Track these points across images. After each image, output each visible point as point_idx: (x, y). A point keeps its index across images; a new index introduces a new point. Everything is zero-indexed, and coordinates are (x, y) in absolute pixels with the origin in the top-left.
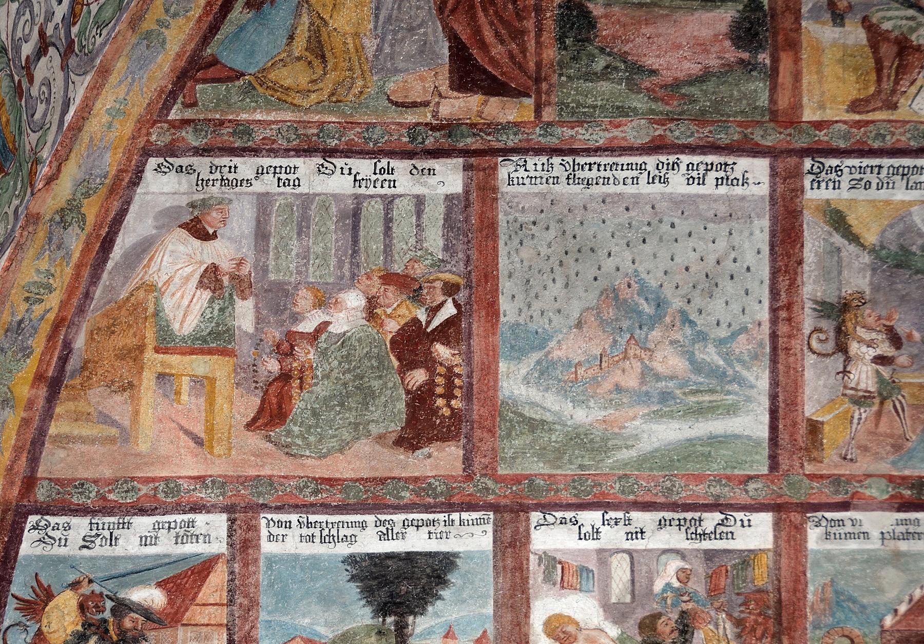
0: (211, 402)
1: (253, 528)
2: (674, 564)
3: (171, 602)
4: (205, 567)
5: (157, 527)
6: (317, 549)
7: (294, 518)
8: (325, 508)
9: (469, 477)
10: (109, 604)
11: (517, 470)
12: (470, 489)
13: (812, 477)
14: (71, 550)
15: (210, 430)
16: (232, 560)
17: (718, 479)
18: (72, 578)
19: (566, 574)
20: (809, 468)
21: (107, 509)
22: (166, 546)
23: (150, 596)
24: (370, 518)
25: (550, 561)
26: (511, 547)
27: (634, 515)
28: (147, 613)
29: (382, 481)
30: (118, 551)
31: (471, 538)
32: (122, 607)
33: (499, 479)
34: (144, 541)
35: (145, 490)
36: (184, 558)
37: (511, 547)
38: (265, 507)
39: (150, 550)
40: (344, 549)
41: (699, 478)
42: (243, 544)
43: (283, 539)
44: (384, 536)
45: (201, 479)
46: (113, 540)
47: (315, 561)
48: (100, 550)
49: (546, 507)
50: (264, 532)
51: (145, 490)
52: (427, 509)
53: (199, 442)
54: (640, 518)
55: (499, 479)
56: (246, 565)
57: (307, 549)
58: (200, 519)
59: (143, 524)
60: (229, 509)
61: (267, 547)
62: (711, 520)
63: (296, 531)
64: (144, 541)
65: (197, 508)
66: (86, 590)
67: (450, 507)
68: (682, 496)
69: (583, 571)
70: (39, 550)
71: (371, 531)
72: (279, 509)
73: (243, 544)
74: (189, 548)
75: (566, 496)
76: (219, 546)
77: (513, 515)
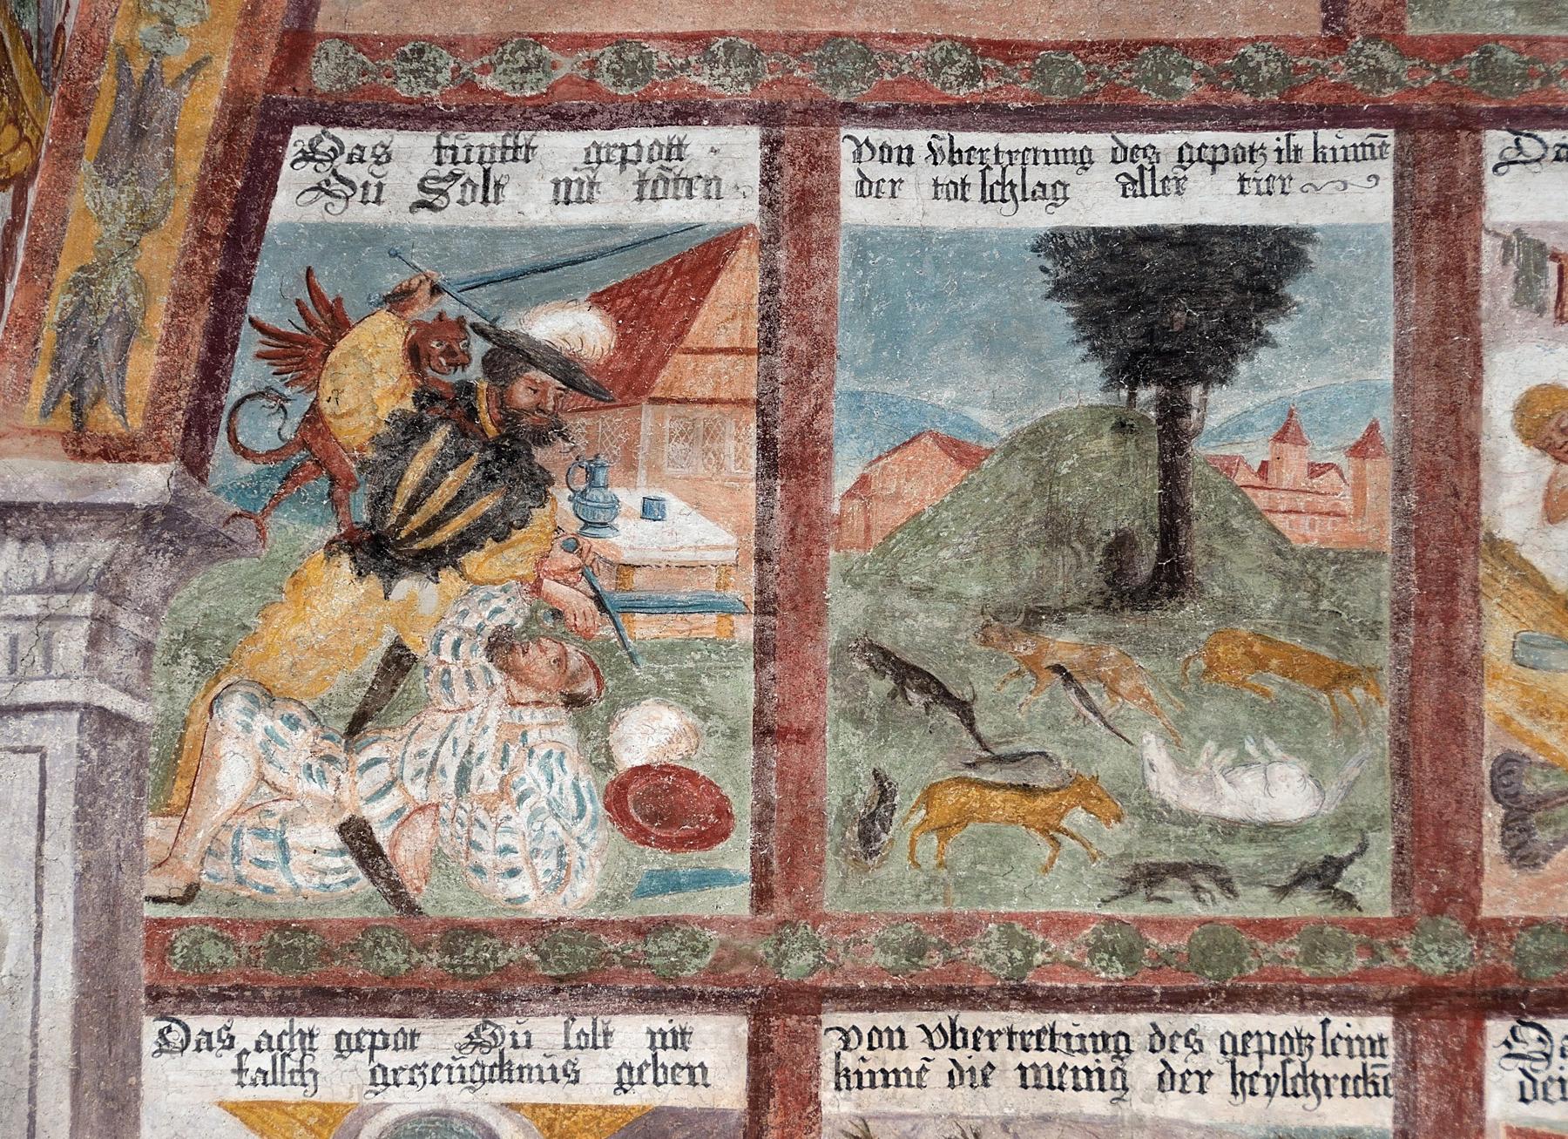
3: (625, 343)
6: (975, 216)
24: (1100, 142)
40: (1037, 218)
44: (1133, 186)
47: (968, 243)
57: (949, 217)
61: (855, 211)
63: (924, 172)
71: (1103, 174)
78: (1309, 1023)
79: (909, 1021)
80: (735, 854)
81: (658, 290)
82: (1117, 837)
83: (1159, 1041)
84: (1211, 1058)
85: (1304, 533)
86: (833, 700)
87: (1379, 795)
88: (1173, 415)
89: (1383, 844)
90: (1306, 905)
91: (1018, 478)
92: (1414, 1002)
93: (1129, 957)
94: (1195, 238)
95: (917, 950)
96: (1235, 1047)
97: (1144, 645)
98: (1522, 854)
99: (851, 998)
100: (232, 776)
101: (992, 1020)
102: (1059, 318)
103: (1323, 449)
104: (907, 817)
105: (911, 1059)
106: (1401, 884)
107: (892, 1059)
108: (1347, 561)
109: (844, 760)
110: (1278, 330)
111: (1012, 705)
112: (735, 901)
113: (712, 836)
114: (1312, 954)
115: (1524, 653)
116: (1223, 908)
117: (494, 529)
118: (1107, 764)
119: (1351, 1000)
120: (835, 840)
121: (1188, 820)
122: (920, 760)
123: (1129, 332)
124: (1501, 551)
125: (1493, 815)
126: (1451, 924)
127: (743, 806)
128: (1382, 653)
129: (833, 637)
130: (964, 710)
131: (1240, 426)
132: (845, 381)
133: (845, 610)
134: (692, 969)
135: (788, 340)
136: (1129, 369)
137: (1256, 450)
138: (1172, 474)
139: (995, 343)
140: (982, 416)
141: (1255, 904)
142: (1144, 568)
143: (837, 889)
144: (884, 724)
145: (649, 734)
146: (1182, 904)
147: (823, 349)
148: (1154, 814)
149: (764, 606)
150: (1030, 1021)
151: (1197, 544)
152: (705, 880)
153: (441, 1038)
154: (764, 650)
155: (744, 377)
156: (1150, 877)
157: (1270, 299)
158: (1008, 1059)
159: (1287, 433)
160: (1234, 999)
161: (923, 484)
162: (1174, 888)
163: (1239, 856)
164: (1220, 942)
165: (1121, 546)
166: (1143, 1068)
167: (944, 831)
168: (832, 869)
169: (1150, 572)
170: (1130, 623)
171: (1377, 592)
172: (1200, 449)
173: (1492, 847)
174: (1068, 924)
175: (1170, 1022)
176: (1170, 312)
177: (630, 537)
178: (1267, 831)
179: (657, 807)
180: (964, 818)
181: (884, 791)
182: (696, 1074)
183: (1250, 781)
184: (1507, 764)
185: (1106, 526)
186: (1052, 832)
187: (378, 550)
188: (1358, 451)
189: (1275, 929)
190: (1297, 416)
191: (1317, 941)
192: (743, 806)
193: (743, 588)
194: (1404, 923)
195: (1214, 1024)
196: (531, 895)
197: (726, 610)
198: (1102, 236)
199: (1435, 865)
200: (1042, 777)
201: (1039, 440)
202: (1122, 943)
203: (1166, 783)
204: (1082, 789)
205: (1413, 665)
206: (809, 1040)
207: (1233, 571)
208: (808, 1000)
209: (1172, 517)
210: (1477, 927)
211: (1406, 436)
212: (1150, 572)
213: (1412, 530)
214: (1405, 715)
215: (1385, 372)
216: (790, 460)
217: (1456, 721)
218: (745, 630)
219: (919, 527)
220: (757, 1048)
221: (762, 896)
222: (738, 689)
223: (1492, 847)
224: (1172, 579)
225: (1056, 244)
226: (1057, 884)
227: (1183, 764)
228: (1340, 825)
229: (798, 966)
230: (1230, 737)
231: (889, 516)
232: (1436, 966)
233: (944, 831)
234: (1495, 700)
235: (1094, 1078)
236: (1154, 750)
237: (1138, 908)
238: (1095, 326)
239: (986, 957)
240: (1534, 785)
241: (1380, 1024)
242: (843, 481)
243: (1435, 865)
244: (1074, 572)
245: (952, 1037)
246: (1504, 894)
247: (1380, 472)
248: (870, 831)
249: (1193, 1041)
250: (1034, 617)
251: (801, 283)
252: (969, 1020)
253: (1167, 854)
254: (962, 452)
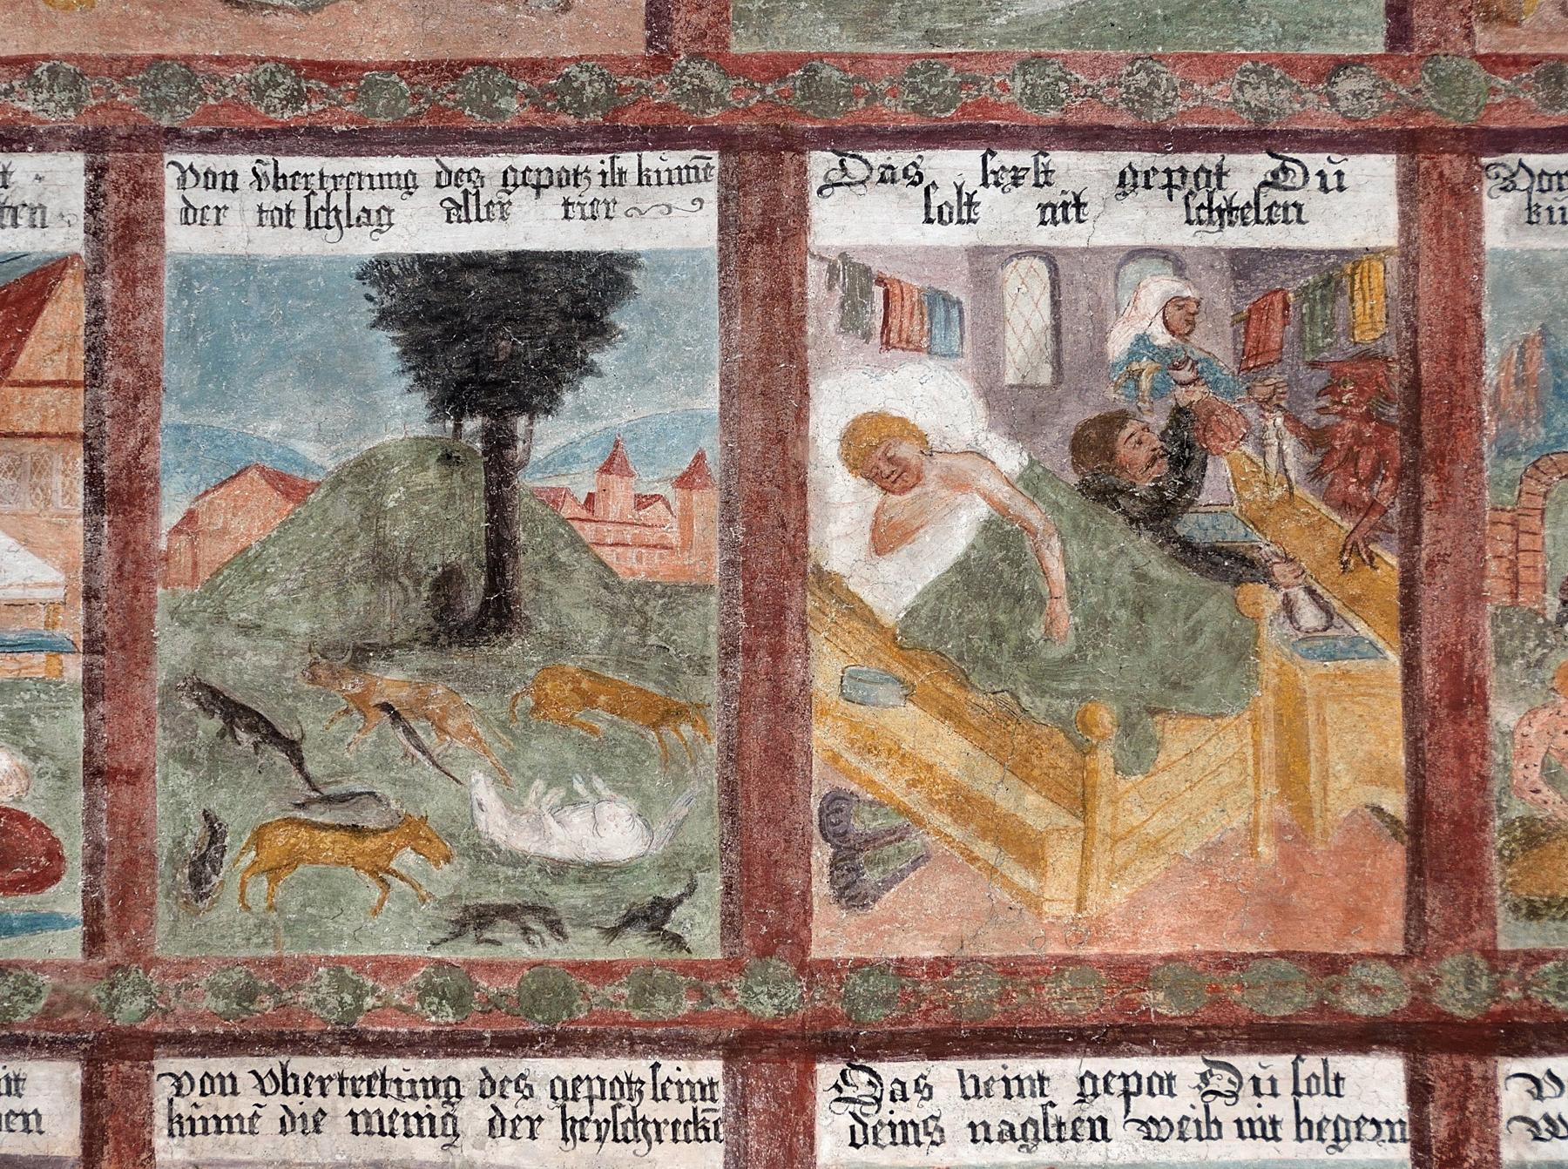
2: (1158, 287)
6: (299, 243)
7: (243, 163)
8: (319, 139)
9: (661, 62)
11: (775, 44)
12: (663, 91)
13: (1493, 62)
16: (95, 271)
17: (1263, 68)
19: (896, 312)
20: (1487, 40)
24: (424, 166)
25: (857, 277)
26: (763, 238)
27: (1060, 159)
29: (453, 70)
31: (667, 217)
33: (733, 67)
37: (763, 238)
38: (174, 136)
40: (363, 245)
41: (1217, 66)
43: (220, 217)
44: (457, 212)
47: (292, 271)
49: (845, 140)
50: (172, 201)
52: (562, 142)
54: (1076, 168)
55: (733, 67)
56: (129, 283)
60: (90, 142)
61: (180, 239)
62: (1246, 172)
63: (248, 199)
67: (614, 138)
68: (1174, 111)
69: (937, 301)
71: (428, 199)
72: (208, 142)
73: (123, 230)
75: (895, 111)
76: (65, 236)
77: (763, 156)
78: (640, 1067)
79: (240, 1067)
80: (67, 897)
82: (447, 878)
83: (490, 1086)
84: (542, 1103)
85: (631, 565)
86: (162, 741)
87: (707, 834)
88: (499, 445)
89: (712, 884)
90: (635, 947)
91: (344, 512)
92: (744, 1046)
93: (459, 1001)
94: (519, 265)
95: (248, 994)
96: (565, 1092)
97: (471, 681)
98: (851, 895)
99: (183, 1043)
101: (323, 1066)
102: (385, 348)
103: (649, 480)
104: (238, 859)
105: (243, 1105)
106: (730, 926)
107: (225, 1106)
108: (674, 595)
109: (175, 800)
110: (603, 358)
111: (341, 744)
112: (66, 945)
113: (44, 879)
114: (642, 996)
115: (852, 687)
116: (552, 951)
118: (435, 805)
119: (681, 1044)
120: (166, 881)
121: (517, 860)
122: (250, 800)
123: (455, 362)
124: (829, 583)
125: (821, 854)
126: (780, 966)
127: (74, 849)
128: (710, 690)
129: (161, 676)
130: (293, 749)
131: (566, 457)
132: (171, 414)
133: (173, 648)
134: (26, 1014)
135: (114, 371)
136: (454, 400)
137: (582, 483)
138: (498, 506)
139: (321, 374)
140: (309, 450)
141: (585, 946)
142: (471, 603)
143: (168, 932)
144: (213, 765)
146: (512, 947)
147: (149, 381)
148: (483, 854)
149: (92, 645)
150: (360, 1066)
151: (525, 576)
152: (37, 923)
154: (93, 690)
155: (70, 410)
156: (478, 919)
157: (595, 327)
158: (339, 1105)
159: (613, 464)
160: (563, 1043)
161: (250, 519)
162: (504, 930)
163: (568, 897)
164: (550, 985)
165: (447, 582)
166: (474, 1114)
167: (274, 872)
168: (164, 911)
169: (477, 608)
170: (458, 660)
171: (704, 626)
172: (527, 481)
173: (821, 887)
174: (397, 968)
175: (501, 1067)
176: (495, 340)
178: (596, 872)
180: (293, 859)
181: (215, 831)
182: (30, 1121)
183: (578, 820)
184: (836, 802)
185: (433, 560)
186: (381, 873)
188: (684, 482)
189: (604, 972)
190: (625, 442)
191: (646, 984)
192: (74, 849)
193: (72, 626)
194: (733, 964)
195: (544, 1068)
197: (55, 649)
198: (427, 263)
199: (765, 908)
200: (371, 818)
201: (365, 473)
202: (451, 986)
203: (495, 822)
204: (411, 830)
205: (740, 702)
206: (142, 1086)
207: (561, 604)
208: (139, 1046)
209: (499, 550)
210: (806, 969)
211: (733, 467)
212: (477, 608)
213: (739, 563)
214: (733, 752)
215: (710, 402)
216: (117, 495)
217: (784, 759)
218: (73, 668)
219: (245, 561)
220: (90, 1094)
221: (94, 941)
222: (68, 729)
223: (821, 887)
224: (499, 614)
225: (379, 271)
226: (388, 927)
227: (512, 804)
228: (669, 865)
229: (131, 1011)
230: (558, 776)
231: (217, 551)
232: (766, 1008)
233: (274, 872)
234: (824, 736)
235: (424, 1124)
236: (483, 790)
237: (468, 951)
238: (420, 356)
239: (316, 1000)
240: (862, 824)
241: (711, 1068)
242: (170, 516)
243: (765, 908)
244: (406, 608)
245: (284, 1081)
246: (833, 935)
247: (707, 503)
248: (200, 872)
249: (524, 1087)
250: (361, 654)
251: (127, 313)
252: (300, 1065)
253: (496, 896)
254: (288, 486)
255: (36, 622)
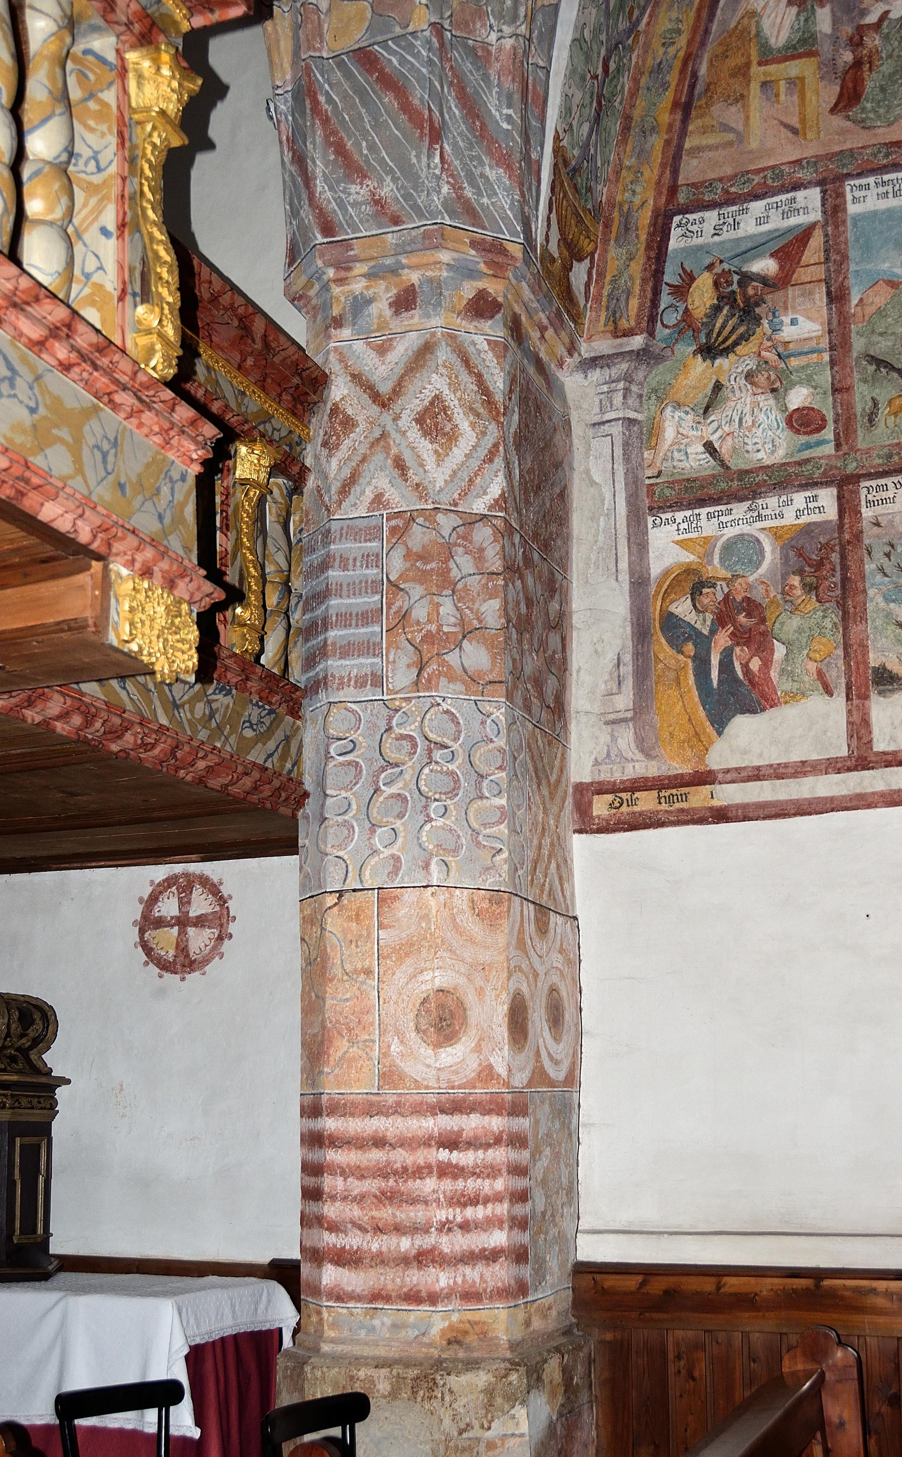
0: (802, 97)
1: (841, 195)
3: (781, 268)
4: (804, 235)
5: (768, 208)
10: (736, 278)
14: (706, 239)
15: (803, 120)
16: (827, 223)
18: (707, 262)
21: (730, 200)
22: (776, 223)
23: (766, 266)
28: (764, 280)
30: (741, 233)
32: (746, 278)
34: (759, 222)
35: (757, 179)
36: (790, 230)
39: (765, 228)
42: (834, 209)
45: (798, 162)
46: (736, 225)
48: (728, 235)
51: (757, 179)
53: (795, 131)
58: (800, 195)
59: (757, 207)
60: (821, 183)
64: (759, 222)
65: (797, 186)
66: (718, 270)
70: (682, 244)
74: (793, 221)
76: (816, 215)
81: (790, 248)
100: (669, 433)
117: (745, 338)
145: (798, 397)
153: (739, 509)
177: (788, 333)
179: (803, 422)
187: (709, 351)
196: (765, 457)
255: (813, 344)
